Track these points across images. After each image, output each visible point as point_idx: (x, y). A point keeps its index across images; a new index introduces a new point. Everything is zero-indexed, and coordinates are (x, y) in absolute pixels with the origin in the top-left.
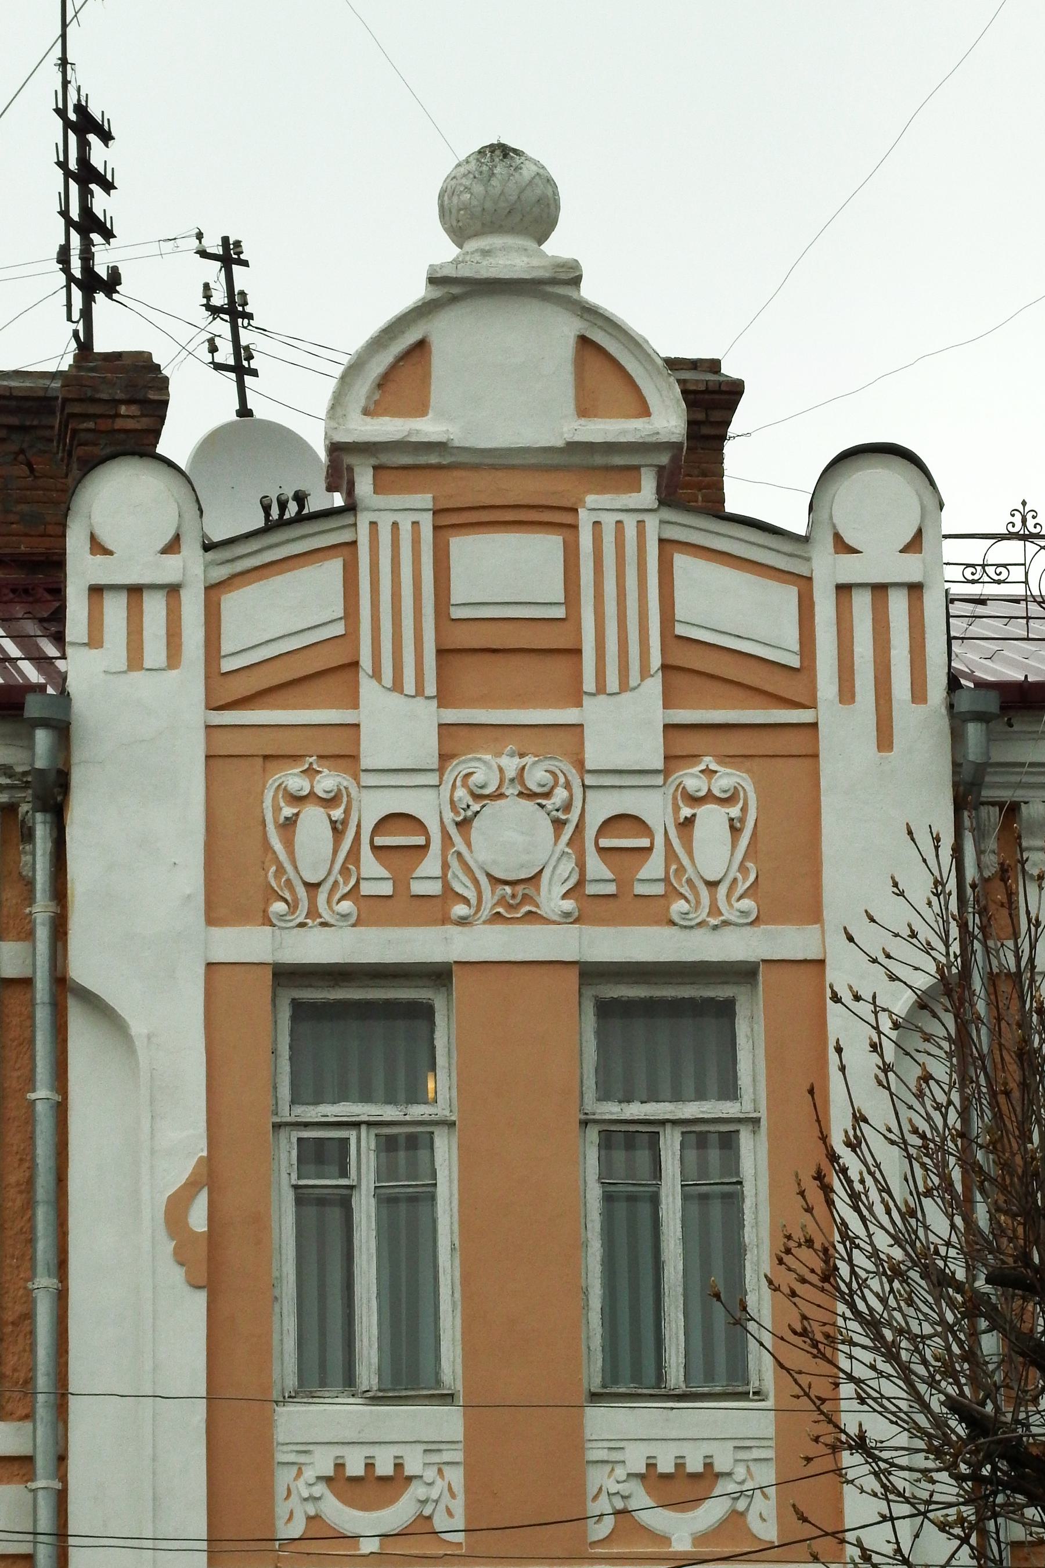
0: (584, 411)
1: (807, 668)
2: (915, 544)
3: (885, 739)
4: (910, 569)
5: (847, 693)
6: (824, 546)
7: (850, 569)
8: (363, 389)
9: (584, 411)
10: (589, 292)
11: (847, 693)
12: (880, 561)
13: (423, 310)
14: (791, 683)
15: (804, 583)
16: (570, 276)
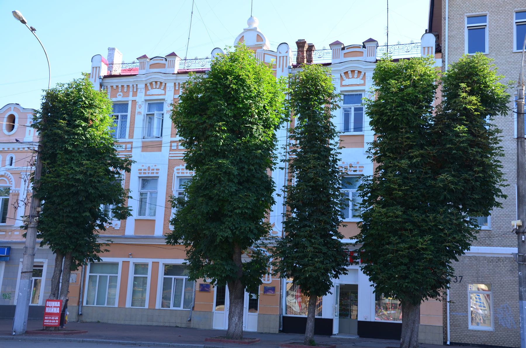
0: (257, 41)
1: (276, 65)
2: (287, 52)
3: (283, 71)
4: (286, 54)
5: (279, 67)
6: (278, 53)
7: (280, 55)
8: (238, 40)
9: (257, 41)
10: (258, 30)
11: (279, 67)
12: (283, 54)
13: (243, 33)
14: (275, 67)
15: (276, 57)
16: (256, 29)
